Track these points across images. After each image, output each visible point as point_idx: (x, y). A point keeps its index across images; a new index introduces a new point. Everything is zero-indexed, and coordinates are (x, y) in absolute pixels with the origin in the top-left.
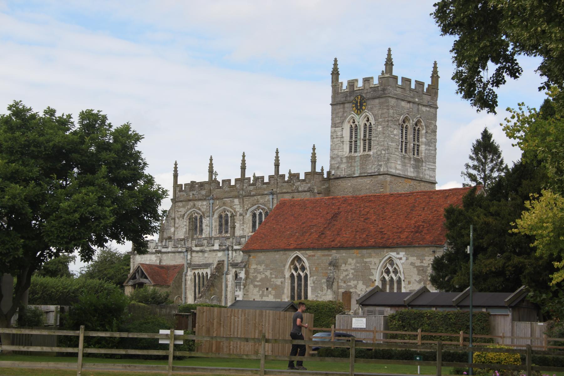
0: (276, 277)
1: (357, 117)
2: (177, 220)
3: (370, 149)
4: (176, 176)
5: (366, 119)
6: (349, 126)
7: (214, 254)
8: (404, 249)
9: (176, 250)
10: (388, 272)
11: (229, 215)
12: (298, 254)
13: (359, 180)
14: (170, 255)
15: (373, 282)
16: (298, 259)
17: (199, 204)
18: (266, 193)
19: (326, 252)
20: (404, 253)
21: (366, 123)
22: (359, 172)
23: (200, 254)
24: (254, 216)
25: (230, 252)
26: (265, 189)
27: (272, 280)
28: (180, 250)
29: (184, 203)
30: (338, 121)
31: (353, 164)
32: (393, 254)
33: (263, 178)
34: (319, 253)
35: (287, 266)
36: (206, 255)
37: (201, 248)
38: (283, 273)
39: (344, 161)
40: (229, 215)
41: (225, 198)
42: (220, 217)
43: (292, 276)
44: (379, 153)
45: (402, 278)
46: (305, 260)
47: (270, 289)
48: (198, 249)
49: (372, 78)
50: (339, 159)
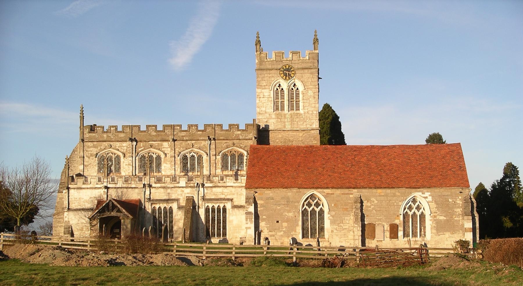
3: (298, 109)
4: (82, 118)
5: (293, 85)
6: (275, 89)
8: (429, 190)
10: (410, 208)
11: (154, 156)
13: (291, 133)
15: (398, 216)
17: (118, 144)
19: (346, 191)
20: (429, 193)
21: (293, 88)
22: (289, 127)
23: (162, 190)
25: (201, 189)
26: (200, 136)
28: (133, 186)
29: (95, 143)
30: (265, 84)
31: (283, 120)
32: (418, 194)
33: (196, 126)
34: (338, 192)
37: (163, 185)
38: (296, 207)
39: (273, 116)
40: (154, 156)
44: (311, 112)
45: (427, 213)
48: (158, 185)
50: (268, 115)
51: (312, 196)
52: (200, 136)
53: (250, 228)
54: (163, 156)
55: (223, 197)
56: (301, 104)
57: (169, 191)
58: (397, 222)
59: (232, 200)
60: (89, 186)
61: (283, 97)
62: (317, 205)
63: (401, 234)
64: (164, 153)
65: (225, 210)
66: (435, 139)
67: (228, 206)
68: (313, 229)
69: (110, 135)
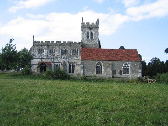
1: (89, 31)
2: (35, 50)
4: (34, 39)
10: (125, 66)
11: (54, 50)
12: (100, 61)
16: (99, 62)
24: (62, 51)
25: (68, 60)
28: (49, 58)
32: (127, 63)
35: (96, 64)
40: (54, 50)
42: (50, 50)
43: (97, 67)
45: (129, 68)
46: (102, 64)
49: (94, 23)
51: (99, 62)
52: (66, 45)
53: (82, 71)
54: (56, 50)
55: (74, 62)
56: (94, 37)
57: (59, 60)
58: (122, 70)
59: (76, 63)
61: (89, 35)
62: (100, 65)
63: (122, 73)
65: (74, 65)
66: (165, 52)
67: (75, 64)
68: (99, 71)
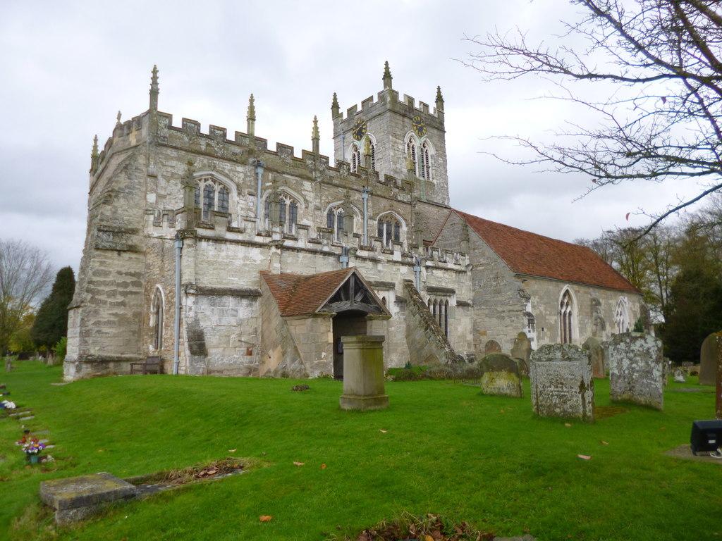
0: (550, 315)
2: (162, 182)
7: (395, 268)
9: (318, 247)
13: (426, 206)
14: (301, 255)
17: (227, 166)
18: (355, 187)
23: (369, 264)
27: (547, 317)
28: (326, 249)
29: (183, 153)
36: (380, 267)
37: (371, 254)
40: (288, 202)
41: (288, 174)
47: (545, 330)
48: (365, 254)
55: (443, 285)
60: (240, 237)
64: (305, 200)
69: (212, 143)
